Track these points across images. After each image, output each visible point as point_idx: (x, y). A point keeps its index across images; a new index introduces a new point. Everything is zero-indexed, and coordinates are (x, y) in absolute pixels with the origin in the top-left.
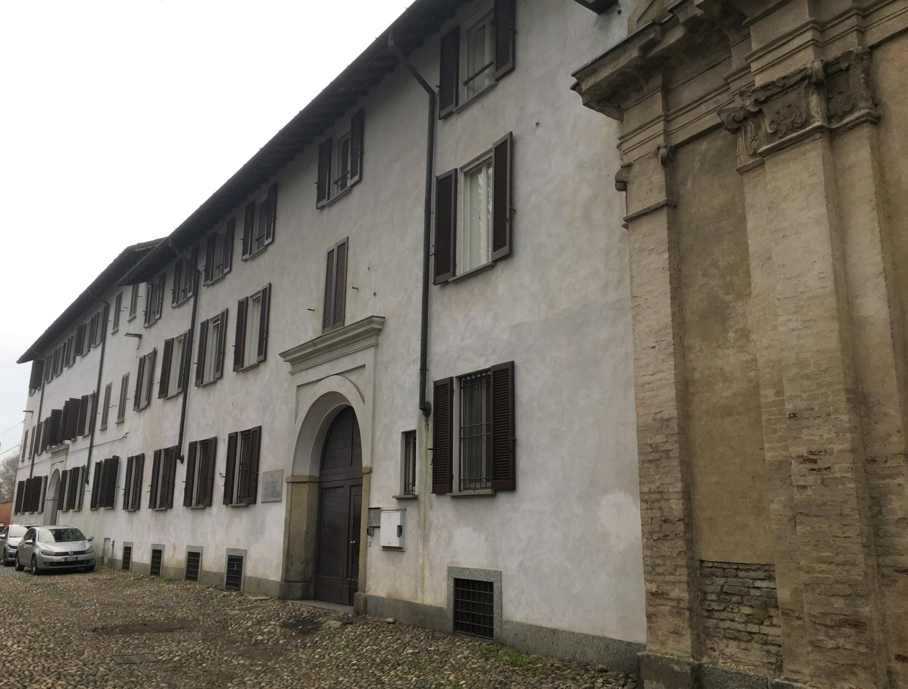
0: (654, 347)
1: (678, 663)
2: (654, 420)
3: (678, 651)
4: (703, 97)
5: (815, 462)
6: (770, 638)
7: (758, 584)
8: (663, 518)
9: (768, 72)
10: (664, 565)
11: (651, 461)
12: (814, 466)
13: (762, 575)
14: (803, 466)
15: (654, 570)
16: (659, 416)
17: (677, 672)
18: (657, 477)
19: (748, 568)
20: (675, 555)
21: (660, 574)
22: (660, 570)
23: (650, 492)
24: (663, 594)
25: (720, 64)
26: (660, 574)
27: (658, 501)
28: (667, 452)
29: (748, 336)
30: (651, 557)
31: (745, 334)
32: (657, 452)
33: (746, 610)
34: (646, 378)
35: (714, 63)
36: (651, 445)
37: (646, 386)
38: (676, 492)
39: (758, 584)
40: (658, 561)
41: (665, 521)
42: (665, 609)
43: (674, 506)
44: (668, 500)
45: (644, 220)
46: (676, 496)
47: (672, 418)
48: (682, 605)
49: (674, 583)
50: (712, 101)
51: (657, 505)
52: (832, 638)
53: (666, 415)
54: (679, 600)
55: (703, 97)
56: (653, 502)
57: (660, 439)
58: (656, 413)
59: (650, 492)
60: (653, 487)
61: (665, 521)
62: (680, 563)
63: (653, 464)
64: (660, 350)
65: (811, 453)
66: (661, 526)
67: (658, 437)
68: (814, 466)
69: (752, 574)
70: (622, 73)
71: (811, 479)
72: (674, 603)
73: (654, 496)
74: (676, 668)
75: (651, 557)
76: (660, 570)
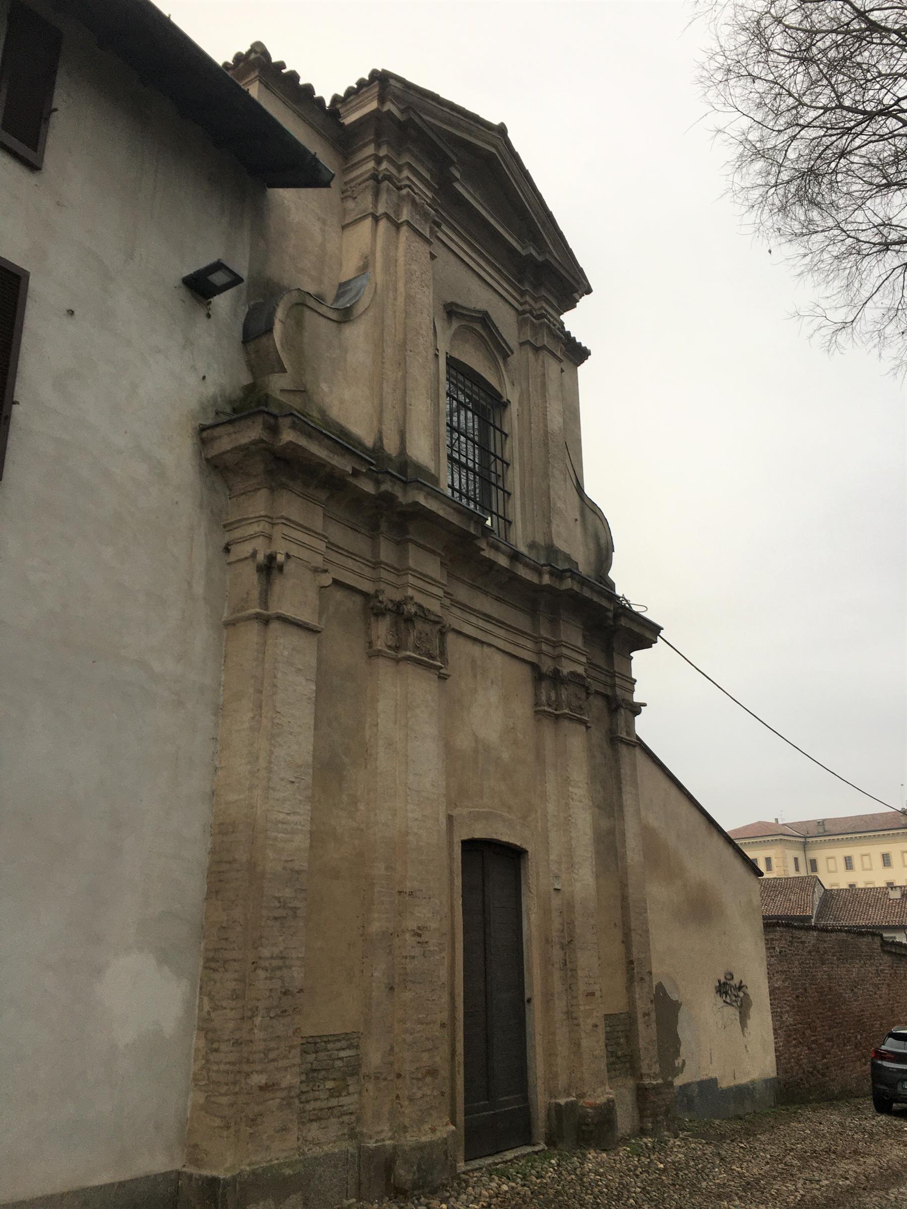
0: (293, 782)
1: (290, 1165)
2: (284, 868)
3: (284, 1151)
4: (352, 553)
5: (420, 935)
6: (345, 1108)
7: (342, 1054)
8: (283, 990)
9: (512, 646)
10: (278, 1049)
11: (276, 918)
12: (419, 939)
13: (344, 1044)
14: (414, 938)
15: (266, 1055)
16: (289, 865)
17: (290, 1176)
18: (281, 939)
19: (336, 1038)
20: (290, 1033)
21: (274, 1060)
22: (272, 1056)
23: (272, 958)
24: (274, 1085)
25: (359, 532)
26: (274, 1060)
27: (280, 968)
28: (294, 910)
29: (356, 803)
30: (264, 1040)
31: (354, 801)
32: (284, 907)
33: (330, 1084)
34: (281, 816)
35: (357, 528)
36: (278, 899)
37: (280, 825)
38: (298, 958)
39: (342, 1054)
40: (273, 1045)
41: (285, 993)
42: (273, 1104)
43: (295, 975)
44: (290, 967)
45: (294, 630)
46: (299, 963)
47: (302, 871)
48: (293, 1094)
49: (286, 1069)
50: (358, 563)
51: (279, 973)
52: (419, 1088)
53: (297, 866)
54: (290, 1088)
55: (339, 547)
56: (274, 969)
57: (288, 893)
58: (287, 861)
59: (272, 958)
60: (276, 951)
61: (285, 993)
62: (295, 1043)
63: (278, 924)
64: (298, 788)
65: (419, 928)
66: (280, 999)
67: (287, 890)
68: (419, 939)
69: (338, 1045)
70: (323, 464)
71: (417, 951)
72: (284, 1094)
73: (276, 963)
74: (288, 1171)
75: (264, 1040)
76: (272, 1056)
